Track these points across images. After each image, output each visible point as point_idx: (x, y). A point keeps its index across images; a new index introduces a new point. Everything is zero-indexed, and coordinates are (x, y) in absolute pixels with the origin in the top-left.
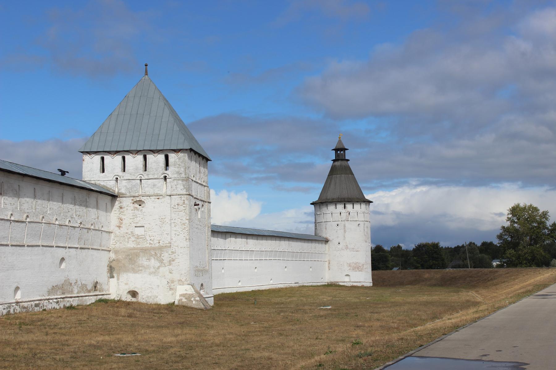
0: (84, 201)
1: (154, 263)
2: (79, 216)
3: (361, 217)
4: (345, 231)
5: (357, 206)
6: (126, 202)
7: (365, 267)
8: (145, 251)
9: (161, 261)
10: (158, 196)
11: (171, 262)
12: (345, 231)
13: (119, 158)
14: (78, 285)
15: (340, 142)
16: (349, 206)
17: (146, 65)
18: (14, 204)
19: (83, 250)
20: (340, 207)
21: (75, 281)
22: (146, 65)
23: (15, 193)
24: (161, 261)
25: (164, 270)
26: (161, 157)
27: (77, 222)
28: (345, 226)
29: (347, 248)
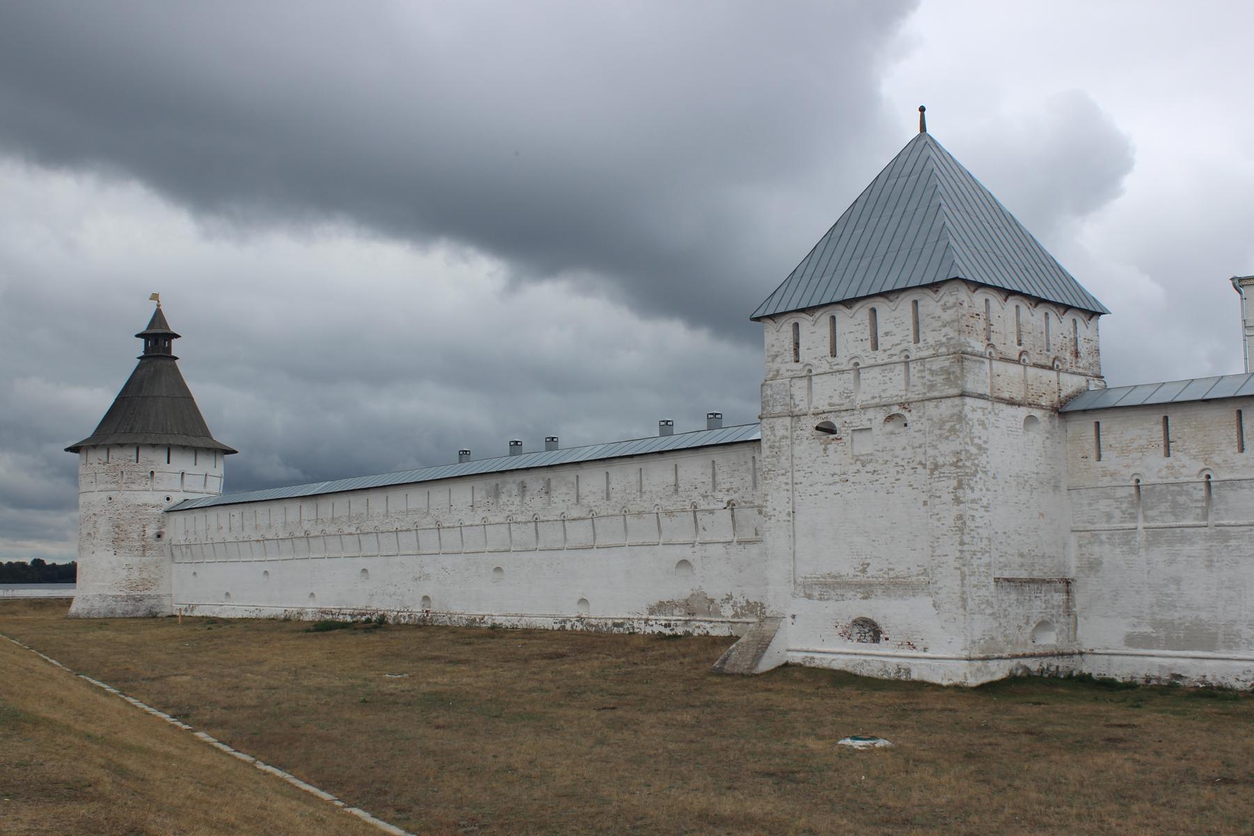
0: (746, 462)
2: (728, 490)
14: (735, 603)
17: (922, 109)
18: (569, 500)
19: (748, 546)
21: (725, 597)
22: (922, 109)
23: (571, 486)
27: (722, 501)
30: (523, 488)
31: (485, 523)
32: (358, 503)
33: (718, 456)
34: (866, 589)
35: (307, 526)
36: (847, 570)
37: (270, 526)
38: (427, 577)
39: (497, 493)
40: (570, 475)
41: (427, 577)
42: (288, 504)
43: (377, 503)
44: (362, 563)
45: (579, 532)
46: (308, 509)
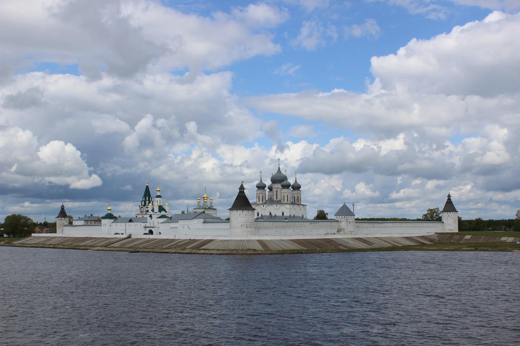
1: (343, 231)
3: (453, 216)
4: (448, 220)
5: (451, 213)
6: (340, 222)
7: (454, 230)
8: (342, 229)
9: (344, 230)
10: (343, 222)
11: (345, 230)
12: (448, 220)
13: (339, 216)
15: (449, 194)
16: (449, 213)
20: (446, 213)
24: (344, 230)
25: (344, 232)
26: (344, 216)
28: (447, 219)
29: (448, 224)
30: (314, 223)
31: (313, 226)
32: (294, 223)
33: (330, 222)
34: (352, 232)
35: (286, 225)
36: (350, 231)
37: (279, 225)
38: (303, 232)
39: (311, 223)
40: (318, 222)
41: (303, 232)
42: (282, 222)
43: (297, 223)
44: (294, 230)
45: (319, 228)
46: (286, 223)
